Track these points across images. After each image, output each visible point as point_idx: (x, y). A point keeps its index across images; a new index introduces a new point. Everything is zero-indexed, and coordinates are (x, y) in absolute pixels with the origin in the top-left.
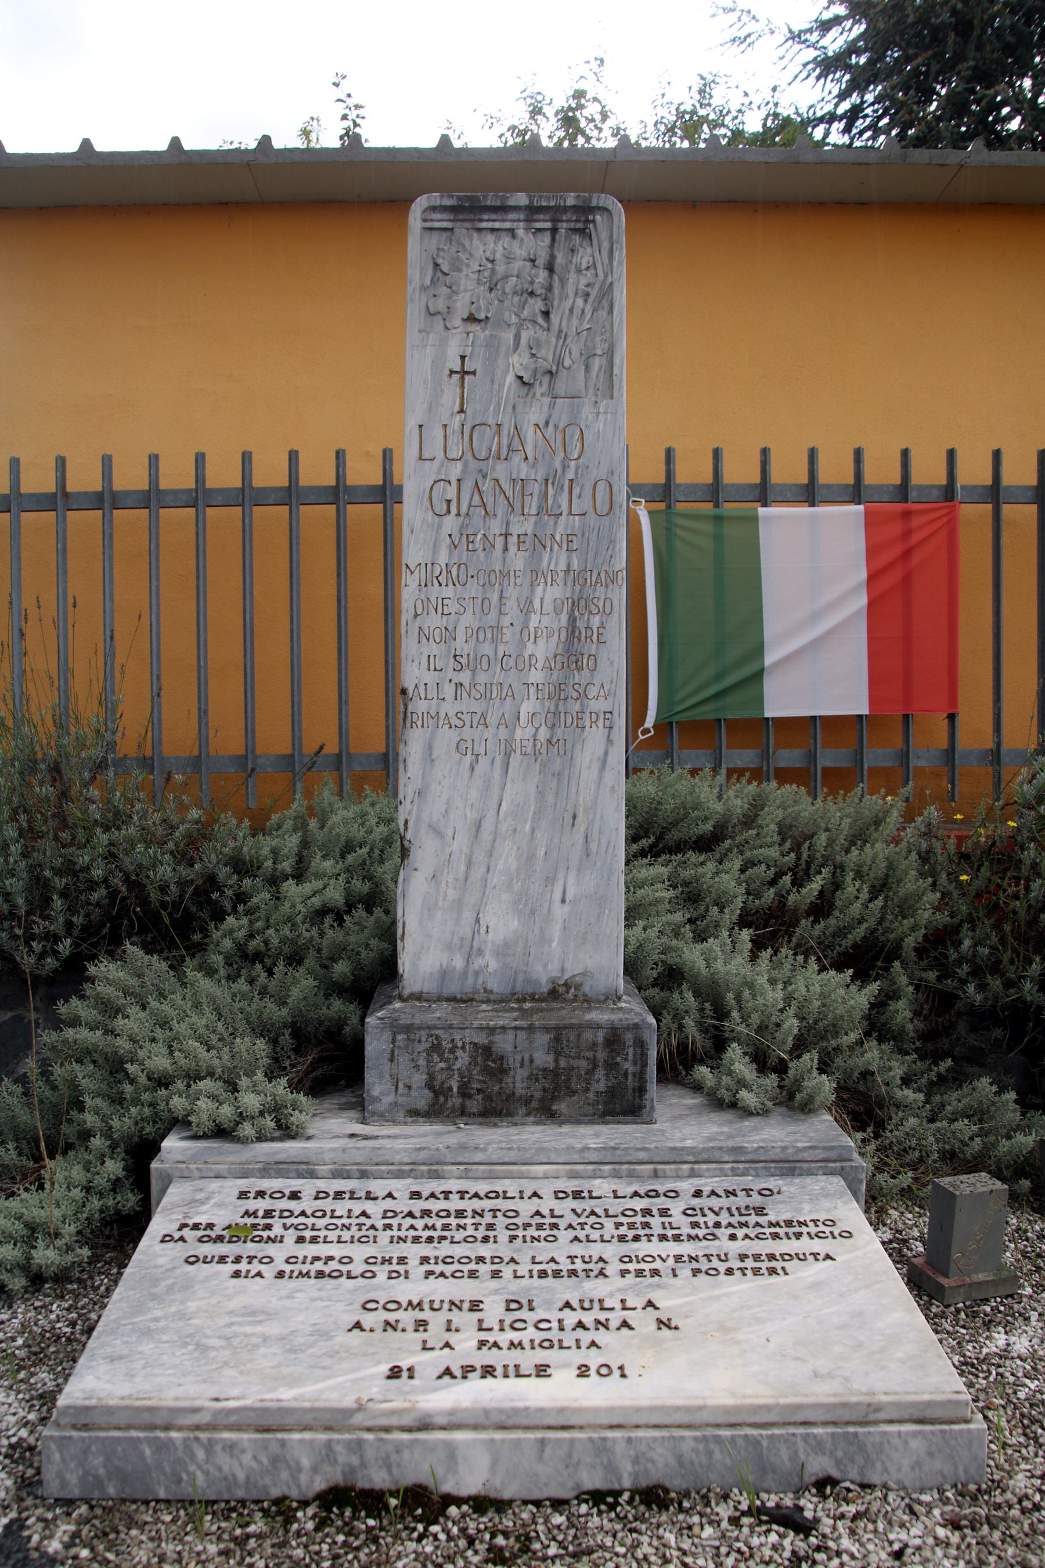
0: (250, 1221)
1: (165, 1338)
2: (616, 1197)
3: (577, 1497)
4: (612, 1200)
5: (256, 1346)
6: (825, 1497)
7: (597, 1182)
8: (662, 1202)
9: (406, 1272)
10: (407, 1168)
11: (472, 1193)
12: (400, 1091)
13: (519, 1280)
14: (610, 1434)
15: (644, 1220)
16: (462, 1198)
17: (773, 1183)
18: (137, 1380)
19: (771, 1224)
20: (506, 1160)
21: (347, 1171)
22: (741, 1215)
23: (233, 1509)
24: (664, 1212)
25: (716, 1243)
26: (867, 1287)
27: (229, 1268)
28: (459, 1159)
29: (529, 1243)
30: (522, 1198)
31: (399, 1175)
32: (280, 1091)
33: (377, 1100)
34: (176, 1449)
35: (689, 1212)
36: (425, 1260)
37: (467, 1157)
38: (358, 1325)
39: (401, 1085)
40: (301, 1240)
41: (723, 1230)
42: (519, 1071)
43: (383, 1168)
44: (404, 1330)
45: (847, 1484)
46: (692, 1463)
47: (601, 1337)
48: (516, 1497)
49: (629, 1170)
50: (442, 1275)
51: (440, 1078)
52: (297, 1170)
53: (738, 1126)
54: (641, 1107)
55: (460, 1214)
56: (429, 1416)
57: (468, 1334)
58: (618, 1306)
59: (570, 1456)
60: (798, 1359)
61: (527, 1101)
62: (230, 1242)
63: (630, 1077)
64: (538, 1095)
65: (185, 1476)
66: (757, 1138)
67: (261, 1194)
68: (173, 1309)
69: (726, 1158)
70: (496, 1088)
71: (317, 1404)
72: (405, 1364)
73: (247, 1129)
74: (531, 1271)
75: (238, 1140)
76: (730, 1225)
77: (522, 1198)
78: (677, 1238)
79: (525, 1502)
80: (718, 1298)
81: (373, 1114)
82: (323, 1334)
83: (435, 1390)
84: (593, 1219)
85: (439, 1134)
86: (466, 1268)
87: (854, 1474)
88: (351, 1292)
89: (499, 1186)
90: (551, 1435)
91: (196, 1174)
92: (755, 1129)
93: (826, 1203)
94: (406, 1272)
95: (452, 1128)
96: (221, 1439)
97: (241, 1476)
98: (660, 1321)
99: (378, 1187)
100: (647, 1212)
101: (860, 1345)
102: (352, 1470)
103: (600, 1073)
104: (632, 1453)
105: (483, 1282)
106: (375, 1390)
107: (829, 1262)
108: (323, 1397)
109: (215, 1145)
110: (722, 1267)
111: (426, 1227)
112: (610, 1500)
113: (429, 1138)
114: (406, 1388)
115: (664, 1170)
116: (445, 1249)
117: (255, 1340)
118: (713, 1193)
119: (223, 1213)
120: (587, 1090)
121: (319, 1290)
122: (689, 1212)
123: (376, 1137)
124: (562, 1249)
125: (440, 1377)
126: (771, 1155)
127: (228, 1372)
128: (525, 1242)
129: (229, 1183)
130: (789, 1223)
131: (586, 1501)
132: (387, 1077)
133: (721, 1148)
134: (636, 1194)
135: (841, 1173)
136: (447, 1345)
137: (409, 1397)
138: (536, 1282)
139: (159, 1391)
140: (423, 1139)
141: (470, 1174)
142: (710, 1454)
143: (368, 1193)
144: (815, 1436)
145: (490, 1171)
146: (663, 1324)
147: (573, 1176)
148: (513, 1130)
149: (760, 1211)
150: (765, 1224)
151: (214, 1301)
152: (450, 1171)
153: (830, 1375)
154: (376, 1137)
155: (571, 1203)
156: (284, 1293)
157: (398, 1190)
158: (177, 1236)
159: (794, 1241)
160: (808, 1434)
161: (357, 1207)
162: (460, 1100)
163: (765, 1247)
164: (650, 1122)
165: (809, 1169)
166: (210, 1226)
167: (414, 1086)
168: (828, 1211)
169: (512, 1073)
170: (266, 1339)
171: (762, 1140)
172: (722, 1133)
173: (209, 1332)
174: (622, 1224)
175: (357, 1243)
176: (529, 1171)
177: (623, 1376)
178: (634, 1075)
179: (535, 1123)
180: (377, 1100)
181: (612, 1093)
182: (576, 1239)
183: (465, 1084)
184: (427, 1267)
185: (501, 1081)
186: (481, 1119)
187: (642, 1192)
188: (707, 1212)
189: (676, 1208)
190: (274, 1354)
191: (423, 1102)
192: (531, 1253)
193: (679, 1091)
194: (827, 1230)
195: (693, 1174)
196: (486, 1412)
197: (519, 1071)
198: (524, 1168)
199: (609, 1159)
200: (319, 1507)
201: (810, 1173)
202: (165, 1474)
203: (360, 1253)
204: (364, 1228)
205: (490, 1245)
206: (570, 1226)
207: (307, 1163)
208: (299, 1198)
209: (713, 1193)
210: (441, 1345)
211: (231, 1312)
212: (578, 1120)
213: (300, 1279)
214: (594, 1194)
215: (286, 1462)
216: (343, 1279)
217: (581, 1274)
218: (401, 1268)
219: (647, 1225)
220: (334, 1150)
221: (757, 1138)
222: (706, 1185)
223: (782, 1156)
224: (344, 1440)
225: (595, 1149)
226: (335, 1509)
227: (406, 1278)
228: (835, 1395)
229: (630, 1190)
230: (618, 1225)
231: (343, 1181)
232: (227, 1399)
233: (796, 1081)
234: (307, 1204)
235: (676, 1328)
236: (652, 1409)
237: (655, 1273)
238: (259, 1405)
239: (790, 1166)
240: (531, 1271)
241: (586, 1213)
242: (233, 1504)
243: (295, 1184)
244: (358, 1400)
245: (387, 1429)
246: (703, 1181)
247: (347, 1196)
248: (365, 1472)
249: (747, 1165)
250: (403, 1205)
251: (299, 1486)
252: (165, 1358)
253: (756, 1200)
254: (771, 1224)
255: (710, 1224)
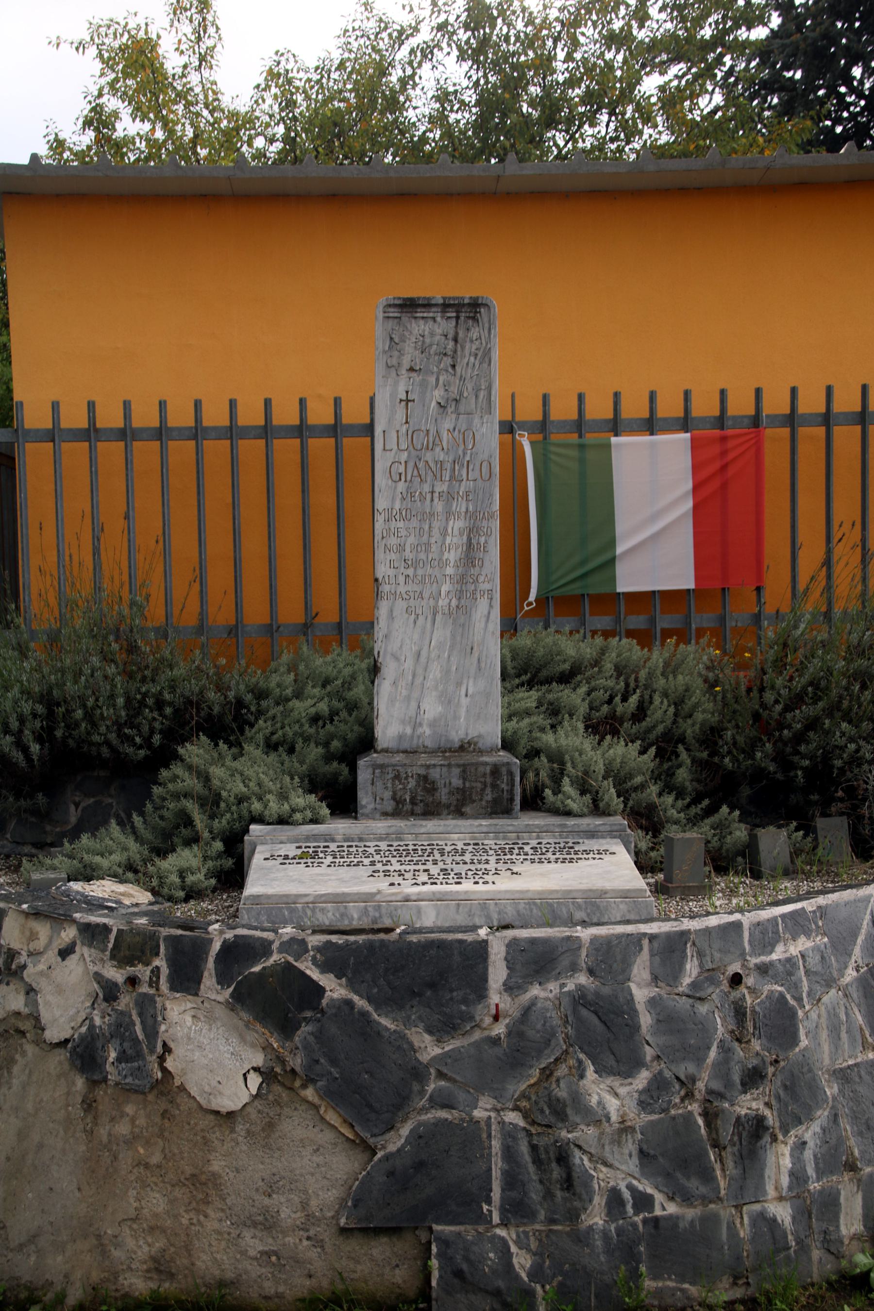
33: (365, 807)
51: (399, 794)
61: (448, 806)
64: (455, 803)
81: (363, 815)
103: (488, 790)
120: (481, 800)
135: (620, 837)
180: (365, 807)
181: (495, 801)
199: (493, 830)
201: (603, 837)
212: (476, 817)
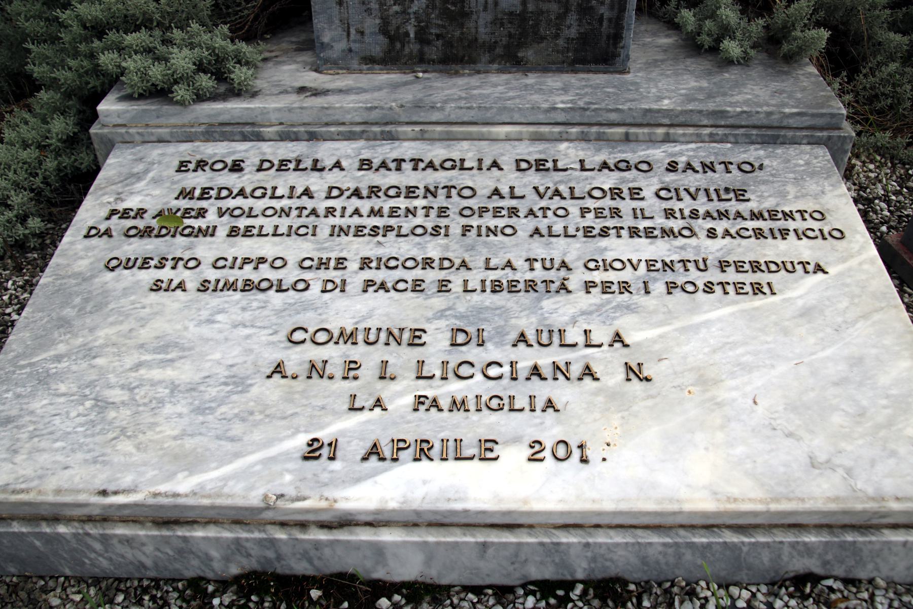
0: (184, 204)
1: (63, 388)
2: (583, 169)
3: (523, 586)
4: (578, 173)
5: (161, 402)
6: (804, 597)
7: (563, 146)
8: (633, 178)
9: (344, 282)
10: (358, 129)
11: (427, 161)
12: (352, 37)
13: (469, 296)
14: (565, 538)
15: (613, 204)
16: (415, 169)
17: (754, 153)
18: (19, 458)
19: (756, 216)
20: (465, 119)
21: (295, 133)
22: (720, 200)
23: (145, 590)
24: (635, 193)
25: (693, 241)
26: (865, 317)
27: (148, 276)
28: (415, 119)
29: (484, 238)
30: (480, 169)
31: (350, 137)
32: (219, 42)
33: (329, 46)
34: (68, 542)
35: (663, 193)
36: (365, 263)
37: (423, 116)
38: (279, 369)
39: (353, 31)
40: (233, 232)
41: (700, 221)
42: (482, 14)
43: (333, 129)
44: (331, 378)
45: (829, 582)
46: (657, 562)
47: (561, 391)
48: (455, 583)
49: (599, 133)
50: (383, 286)
51: (394, 22)
52: (242, 133)
53: (717, 79)
54: (615, 55)
55: (410, 192)
56: (351, 514)
57: (405, 383)
58: (581, 340)
59: (516, 555)
60: (790, 435)
61: (491, 48)
62: (158, 236)
63: (605, 23)
64: (505, 40)
65: (87, 561)
66: (739, 98)
67: (201, 165)
68: (80, 340)
69: (705, 122)
70: (457, 33)
71: (219, 502)
72: (325, 435)
73: (180, 92)
74: (483, 282)
75: (171, 102)
76: (708, 214)
77: (480, 169)
78: (649, 233)
79: (467, 589)
80: (696, 328)
81: (326, 61)
82: (238, 383)
83: (358, 480)
84: (556, 202)
85: (395, 86)
86: (410, 276)
87: (840, 571)
88: (278, 312)
89: (457, 151)
90: (495, 537)
91: (138, 138)
92: (737, 85)
93: (812, 186)
94: (344, 282)
95: (410, 77)
96: (115, 536)
97: (148, 562)
98: (628, 368)
99: (327, 152)
100: (616, 193)
101: (861, 414)
102: (268, 561)
103: (572, 18)
104: (589, 554)
105: (428, 297)
106: (288, 478)
107: (820, 275)
108: (226, 490)
109: (153, 108)
110: (701, 279)
111: (373, 212)
112: (560, 593)
113: (382, 94)
114: (325, 477)
115: (636, 135)
116: (392, 247)
117: (163, 392)
118: (689, 166)
119: (157, 192)
120: (557, 36)
121: (244, 309)
122: (663, 193)
123: (325, 92)
124: (518, 249)
125: (365, 459)
126: (754, 121)
127: (126, 446)
128: (479, 235)
129: (171, 149)
130: (773, 215)
131: (533, 593)
132: (337, 22)
133: (700, 112)
134: (605, 165)
135: (826, 143)
136: (378, 403)
137: (327, 494)
138: (489, 299)
139: (40, 477)
140: (376, 95)
141: (426, 136)
142: (679, 556)
143: (316, 161)
144: (805, 544)
145: (447, 132)
146: (634, 372)
147: (537, 138)
148: (474, 81)
149: (740, 195)
150: (746, 214)
151: (125, 327)
152: (405, 132)
153: (829, 465)
154: (325, 92)
155: (534, 178)
156: (205, 314)
157: (348, 157)
158: (103, 228)
159: (779, 242)
160: (798, 543)
161: (300, 181)
162: (418, 47)
163: (748, 250)
164: (624, 71)
165: (793, 137)
166: (141, 213)
167: (367, 32)
168: (816, 197)
169: (474, 17)
170: (174, 388)
171: (746, 102)
172: (701, 89)
173: (112, 379)
174: (588, 210)
175: (294, 236)
176: (490, 132)
177: (584, 460)
178: (610, 20)
179: (501, 71)
180: (329, 46)
181: (584, 40)
182: (537, 231)
183: (422, 28)
184: (368, 274)
185: (462, 26)
186: (441, 67)
187: (611, 163)
188: (683, 194)
189: (649, 185)
190: (180, 415)
191: (378, 49)
192: (485, 253)
193: (653, 26)
194: (816, 225)
195: (667, 139)
196: (417, 513)
197: (482, 14)
198: (485, 129)
199: (578, 119)
200: (236, 593)
201: (794, 142)
202: (64, 559)
203: (296, 249)
204: (305, 212)
205: (441, 240)
206: (531, 212)
207: (253, 124)
208: (241, 170)
209: (689, 166)
210: (372, 402)
211: (142, 346)
212: (545, 68)
213: (226, 293)
214: (560, 165)
215: (193, 553)
216: (272, 292)
217: (541, 287)
218: (336, 275)
219: (616, 213)
220: (279, 110)
221: (739, 98)
222: (681, 154)
223: (765, 122)
224: (255, 539)
225: (563, 109)
226: (253, 598)
227: (343, 291)
228: (836, 499)
229: (599, 158)
230: (584, 211)
231: (290, 145)
232: (116, 493)
233: (785, 27)
234: (247, 179)
235: (648, 379)
236: (615, 514)
237: (625, 287)
238: (151, 501)
239: (772, 133)
240: (483, 282)
241: (549, 193)
242: (146, 583)
243: (239, 150)
244: (266, 497)
245: (303, 525)
246: (678, 148)
247: (292, 166)
248: (283, 562)
249: (727, 131)
250: (348, 180)
251: (213, 570)
252: (57, 421)
253: (735, 178)
254: (756, 216)
255: (687, 213)
